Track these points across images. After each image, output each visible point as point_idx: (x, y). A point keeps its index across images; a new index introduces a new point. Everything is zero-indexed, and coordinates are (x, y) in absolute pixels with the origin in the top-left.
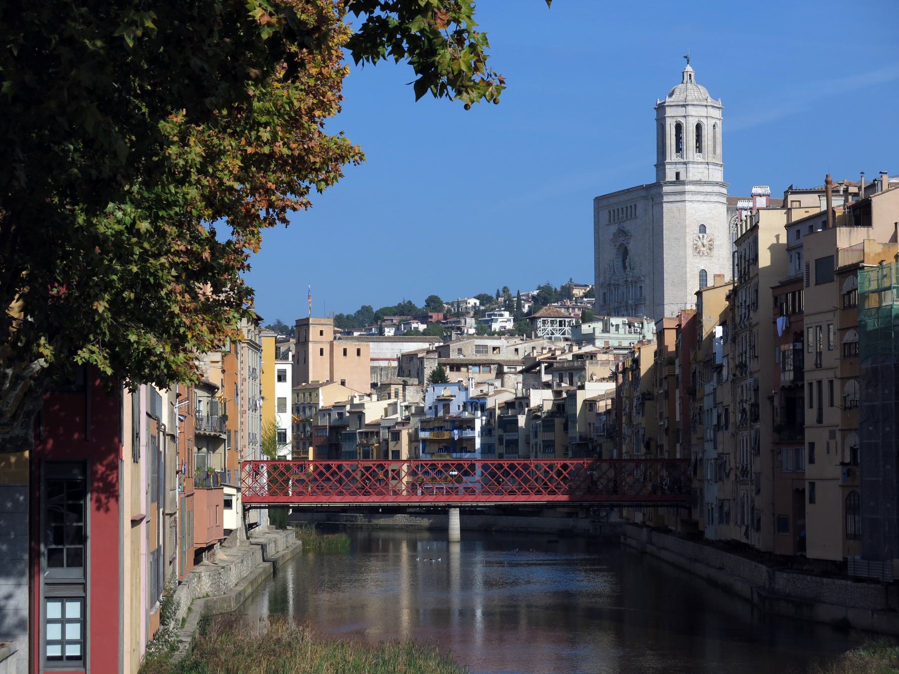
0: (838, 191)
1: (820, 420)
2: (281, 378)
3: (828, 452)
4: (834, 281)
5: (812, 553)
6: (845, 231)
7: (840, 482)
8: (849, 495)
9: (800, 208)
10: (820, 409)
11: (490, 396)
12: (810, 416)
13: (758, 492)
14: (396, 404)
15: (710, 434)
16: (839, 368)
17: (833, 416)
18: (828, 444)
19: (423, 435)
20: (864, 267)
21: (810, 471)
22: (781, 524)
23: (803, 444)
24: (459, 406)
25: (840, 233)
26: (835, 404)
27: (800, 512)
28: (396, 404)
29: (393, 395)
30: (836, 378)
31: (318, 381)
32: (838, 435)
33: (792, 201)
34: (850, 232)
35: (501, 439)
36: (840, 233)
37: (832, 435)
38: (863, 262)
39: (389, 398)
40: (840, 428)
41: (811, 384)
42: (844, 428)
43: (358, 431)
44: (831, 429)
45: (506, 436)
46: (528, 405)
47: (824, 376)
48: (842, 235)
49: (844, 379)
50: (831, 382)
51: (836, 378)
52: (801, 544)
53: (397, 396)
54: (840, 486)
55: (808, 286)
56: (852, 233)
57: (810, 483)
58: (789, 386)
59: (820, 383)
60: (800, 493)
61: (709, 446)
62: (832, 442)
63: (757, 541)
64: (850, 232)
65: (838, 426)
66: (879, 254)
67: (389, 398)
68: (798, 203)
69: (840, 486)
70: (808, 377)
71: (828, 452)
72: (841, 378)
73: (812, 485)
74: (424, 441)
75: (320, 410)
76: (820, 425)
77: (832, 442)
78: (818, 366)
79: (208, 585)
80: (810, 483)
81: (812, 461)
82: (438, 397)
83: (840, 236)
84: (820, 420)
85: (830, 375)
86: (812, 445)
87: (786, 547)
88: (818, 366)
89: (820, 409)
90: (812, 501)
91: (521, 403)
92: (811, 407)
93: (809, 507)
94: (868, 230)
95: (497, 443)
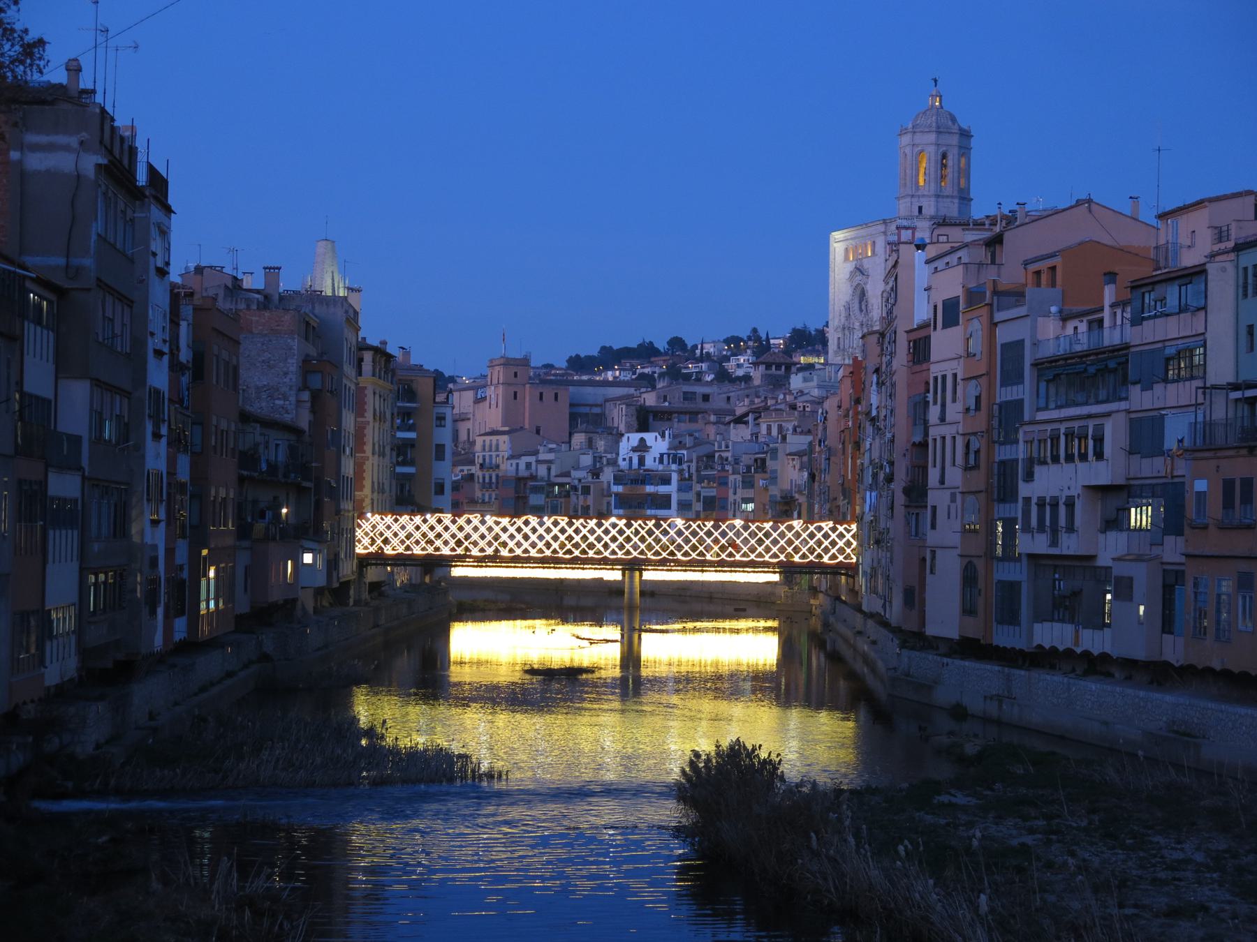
0: (984, 225)
1: (942, 482)
3: (949, 518)
4: (957, 324)
5: (931, 630)
7: (958, 551)
8: (966, 567)
9: (948, 242)
10: (943, 468)
12: (933, 475)
16: (961, 424)
17: (955, 476)
18: (949, 507)
23: (926, 507)
24: (655, 458)
26: (956, 464)
30: (958, 433)
31: (310, 421)
32: (959, 497)
33: (938, 235)
35: (698, 494)
37: (953, 497)
40: (960, 490)
41: (935, 440)
42: (964, 490)
44: (953, 491)
45: (705, 492)
47: (947, 431)
50: (954, 438)
51: (958, 433)
52: (923, 622)
54: (959, 555)
55: (935, 328)
57: (932, 551)
58: (920, 442)
59: (944, 438)
62: (953, 506)
64: (978, 271)
65: (958, 488)
68: (945, 237)
69: (959, 555)
70: (934, 432)
71: (949, 518)
72: (962, 435)
73: (933, 553)
74: (617, 495)
76: (943, 486)
77: (953, 506)
78: (942, 419)
80: (932, 551)
81: (933, 526)
84: (942, 482)
86: (934, 508)
88: (942, 419)
89: (943, 468)
90: (932, 572)
92: (935, 466)
93: (929, 578)
95: (694, 500)
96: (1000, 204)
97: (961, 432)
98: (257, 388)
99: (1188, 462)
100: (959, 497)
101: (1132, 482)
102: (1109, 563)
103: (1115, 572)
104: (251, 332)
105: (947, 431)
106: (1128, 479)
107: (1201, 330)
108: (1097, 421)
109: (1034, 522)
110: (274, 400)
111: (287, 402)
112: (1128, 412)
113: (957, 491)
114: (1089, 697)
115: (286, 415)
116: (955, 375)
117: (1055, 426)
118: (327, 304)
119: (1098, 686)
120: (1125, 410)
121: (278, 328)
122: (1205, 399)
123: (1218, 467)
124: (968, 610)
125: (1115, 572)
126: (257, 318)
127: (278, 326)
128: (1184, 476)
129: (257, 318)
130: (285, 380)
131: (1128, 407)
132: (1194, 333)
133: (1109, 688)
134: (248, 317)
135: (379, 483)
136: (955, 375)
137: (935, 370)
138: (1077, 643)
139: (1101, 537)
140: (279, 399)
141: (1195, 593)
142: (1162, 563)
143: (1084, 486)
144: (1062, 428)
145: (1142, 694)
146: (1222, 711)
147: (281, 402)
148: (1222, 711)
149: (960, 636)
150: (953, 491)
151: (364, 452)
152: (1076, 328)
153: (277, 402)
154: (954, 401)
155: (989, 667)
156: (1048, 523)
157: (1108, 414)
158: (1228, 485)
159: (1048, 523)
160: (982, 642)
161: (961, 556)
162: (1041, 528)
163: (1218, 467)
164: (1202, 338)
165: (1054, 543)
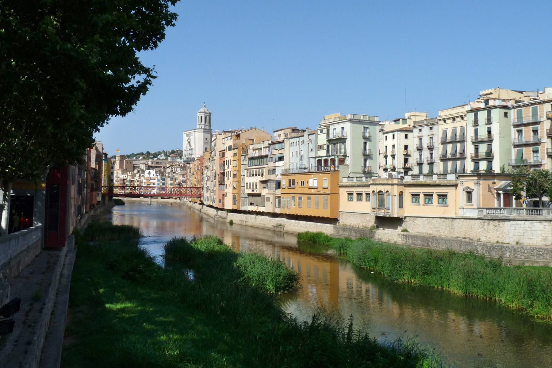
1: (228, 180)
5: (225, 208)
12: (226, 178)
13: (215, 195)
15: (205, 182)
17: (231, 179)
21: (226, 190)
22: (220, 201)
23: (224, 185)
27: (223, 199)
32: (232, 183)
35: (161, 182)
37: (231, 183)
47: (229, 170)
59: (228, 172)
60: (224, 195)
61: (205, 185)
63: (214, 205)
70: (226, 171)
78: (228, 168)
81: (226, 188)
85: (231, 170)
86: (226, 185)
87: (220, 207)
88: (228, 168)
90: (226, 197)
102: (265, 195)
103: (266, 196)
105: (228, 170)
109: (249, 187)
116: (231, 160)
124: (234, 203)
125: (266, 196)
136: (231, 160)
137: (226, 159)
139: (262, 190)
154: (231, 164)
156: (251, 187)
157: (264, 168)
158: (290, 181)
159: (251, 187)
162: (250, 188)
165: (253, 191)
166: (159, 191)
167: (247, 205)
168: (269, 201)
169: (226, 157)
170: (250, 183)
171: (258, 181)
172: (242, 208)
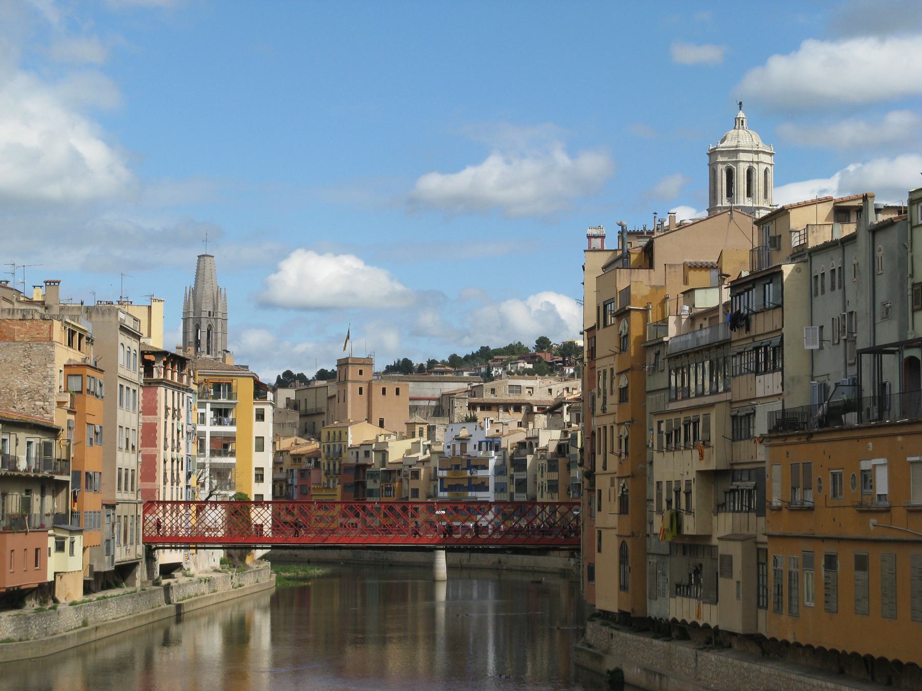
1: (605, 468)
2: (260, 416)
3: (610, 501)
6: (625, 273)
7: (616, 532)
10: (606, 455)
11: (504, 436)
14: (419, 442)
17: (613, 463)
18: (610, 490)
19: (442, 474)
20: (630, 310)
23: (594, 491)
24: (475, 446)
25: (620, 275)
28: (419, 442)
29: (417, 433)
32: (616, 481)
34: (630, 275)
35: (512, 477)
36: (620, 275)
38: (629, 304)
39: (413, 436)
42: (620, 476)
43: (381, 469)
45: (517, 475)
46: (537, 445)
47: (607, 421)
48: (622, 277)
49: (620, 425)
51: (614, 423)
53: (421, 434)
54: (618, 536)
56: (633, 274)
59: (605, 427)
64: (630, 275)
65: (616, 473)
66: (646, 297)
67: (413, 436)
71: (610, 501)
73: (600, 532)
74: (442, 479)
75: (349, 448)
76: (605, 472)
77: (612, 489)
79: (10, 630)
82: (456, 436)
83: (620, 278)
84: (605, 468)
86: (600, 491)
91: (527, 445)
94: (649, 273)
96: (655, 213)
97: (617, 422)
98: (19, 390)
99: (768, 448)
100: (616, 481)
101: (736, 467)
104: (14, 341)
106: (732, 464)
107: (779, 327)
108: (705, 412)
110: (35, 401)
111: (46, 403)
112: (731, 402)
113: (615, 476)
114: (710, 667)
115: (45, 415)
116: (612, 370)
117: (677, 416)
118: (103, 314)
119: (716, 656)
120: (726, 401)
121: (38, 336)
122: (783, 390)
123: (788, 453)
125: (721, 551)
126: (19, 328)
127: (37, 334)
128: (764, 462)
129: (19, 328)
130: (44, 383)
131: (729, 398)
132: (774, 329)
133: (722, 658)
134: (11, 326)
135: (173, 474)
136: (612, 370)
138: (698, 616)
139: (715, 518)
140: (40, 400)
141: (775, 570)
142: (756, 543)
143: (698, 472)
144: (682, 417)
145: (746, 664)
146: (800, 682)
147: (42, 403)
148: (800, 682)
149: (619, 610)
150: (612, 476)
151: (155, 446)
152: (701, 325)
153: (37, 403)
155: (642, 638)
157: (712, 405)
158: (794, 467)
160: (632, 615)
161: (618, 536)
163: (788, 453)
164: (779, 333)
166: (507, 517)
167: (668, 595)
168: (730, 575)
169: (597, 356)
170: (669, 483)
171: (692, 476)
172: (655, 610)
